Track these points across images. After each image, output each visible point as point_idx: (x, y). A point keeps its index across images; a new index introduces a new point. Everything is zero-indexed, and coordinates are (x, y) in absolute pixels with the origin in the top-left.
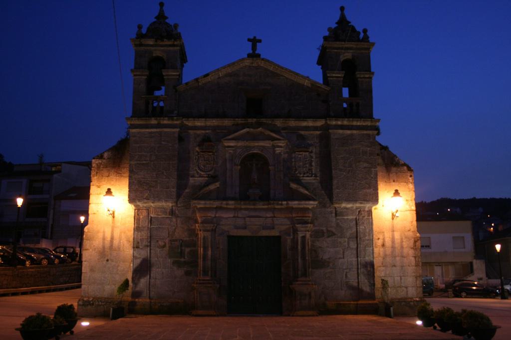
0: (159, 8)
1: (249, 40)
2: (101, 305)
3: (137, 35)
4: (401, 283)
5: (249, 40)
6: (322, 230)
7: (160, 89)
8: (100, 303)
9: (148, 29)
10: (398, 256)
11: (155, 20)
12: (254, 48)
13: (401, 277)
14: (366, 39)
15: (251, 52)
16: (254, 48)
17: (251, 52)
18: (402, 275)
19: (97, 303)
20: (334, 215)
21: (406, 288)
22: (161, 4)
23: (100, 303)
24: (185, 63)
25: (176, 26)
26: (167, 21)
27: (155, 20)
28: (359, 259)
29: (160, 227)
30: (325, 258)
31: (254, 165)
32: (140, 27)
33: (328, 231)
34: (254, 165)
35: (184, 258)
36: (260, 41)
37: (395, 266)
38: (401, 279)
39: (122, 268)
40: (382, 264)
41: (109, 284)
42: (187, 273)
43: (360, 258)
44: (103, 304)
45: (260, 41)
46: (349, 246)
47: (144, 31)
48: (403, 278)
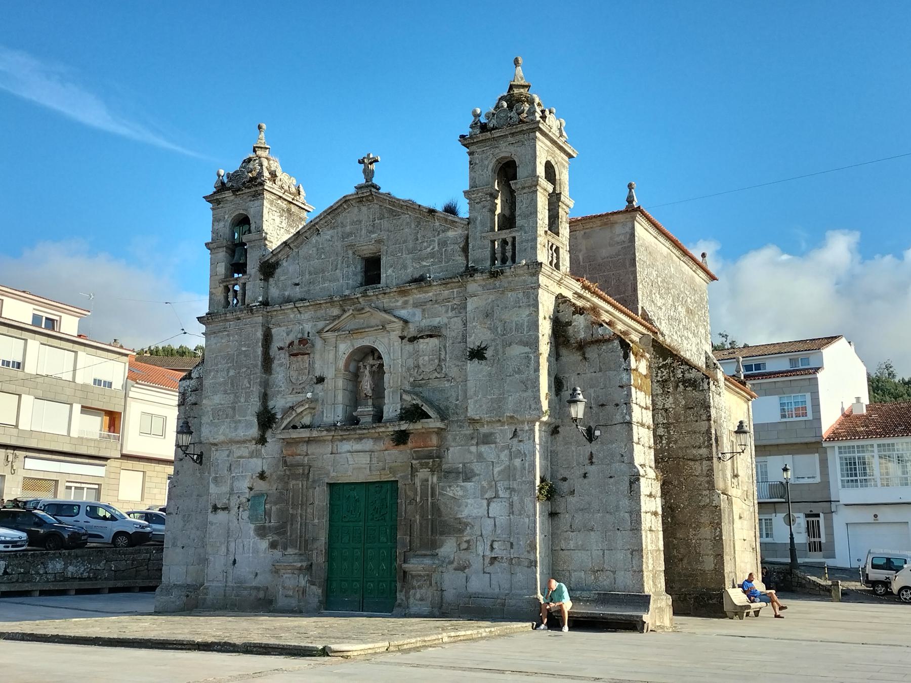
12: (369, 174)
17: (362, 181)
18: (606, 548)
20: (474, 442)
21: (614, 572)
29: (242, 476)
38: (603, 554)
42: (273, 545)
46: (497, 496)
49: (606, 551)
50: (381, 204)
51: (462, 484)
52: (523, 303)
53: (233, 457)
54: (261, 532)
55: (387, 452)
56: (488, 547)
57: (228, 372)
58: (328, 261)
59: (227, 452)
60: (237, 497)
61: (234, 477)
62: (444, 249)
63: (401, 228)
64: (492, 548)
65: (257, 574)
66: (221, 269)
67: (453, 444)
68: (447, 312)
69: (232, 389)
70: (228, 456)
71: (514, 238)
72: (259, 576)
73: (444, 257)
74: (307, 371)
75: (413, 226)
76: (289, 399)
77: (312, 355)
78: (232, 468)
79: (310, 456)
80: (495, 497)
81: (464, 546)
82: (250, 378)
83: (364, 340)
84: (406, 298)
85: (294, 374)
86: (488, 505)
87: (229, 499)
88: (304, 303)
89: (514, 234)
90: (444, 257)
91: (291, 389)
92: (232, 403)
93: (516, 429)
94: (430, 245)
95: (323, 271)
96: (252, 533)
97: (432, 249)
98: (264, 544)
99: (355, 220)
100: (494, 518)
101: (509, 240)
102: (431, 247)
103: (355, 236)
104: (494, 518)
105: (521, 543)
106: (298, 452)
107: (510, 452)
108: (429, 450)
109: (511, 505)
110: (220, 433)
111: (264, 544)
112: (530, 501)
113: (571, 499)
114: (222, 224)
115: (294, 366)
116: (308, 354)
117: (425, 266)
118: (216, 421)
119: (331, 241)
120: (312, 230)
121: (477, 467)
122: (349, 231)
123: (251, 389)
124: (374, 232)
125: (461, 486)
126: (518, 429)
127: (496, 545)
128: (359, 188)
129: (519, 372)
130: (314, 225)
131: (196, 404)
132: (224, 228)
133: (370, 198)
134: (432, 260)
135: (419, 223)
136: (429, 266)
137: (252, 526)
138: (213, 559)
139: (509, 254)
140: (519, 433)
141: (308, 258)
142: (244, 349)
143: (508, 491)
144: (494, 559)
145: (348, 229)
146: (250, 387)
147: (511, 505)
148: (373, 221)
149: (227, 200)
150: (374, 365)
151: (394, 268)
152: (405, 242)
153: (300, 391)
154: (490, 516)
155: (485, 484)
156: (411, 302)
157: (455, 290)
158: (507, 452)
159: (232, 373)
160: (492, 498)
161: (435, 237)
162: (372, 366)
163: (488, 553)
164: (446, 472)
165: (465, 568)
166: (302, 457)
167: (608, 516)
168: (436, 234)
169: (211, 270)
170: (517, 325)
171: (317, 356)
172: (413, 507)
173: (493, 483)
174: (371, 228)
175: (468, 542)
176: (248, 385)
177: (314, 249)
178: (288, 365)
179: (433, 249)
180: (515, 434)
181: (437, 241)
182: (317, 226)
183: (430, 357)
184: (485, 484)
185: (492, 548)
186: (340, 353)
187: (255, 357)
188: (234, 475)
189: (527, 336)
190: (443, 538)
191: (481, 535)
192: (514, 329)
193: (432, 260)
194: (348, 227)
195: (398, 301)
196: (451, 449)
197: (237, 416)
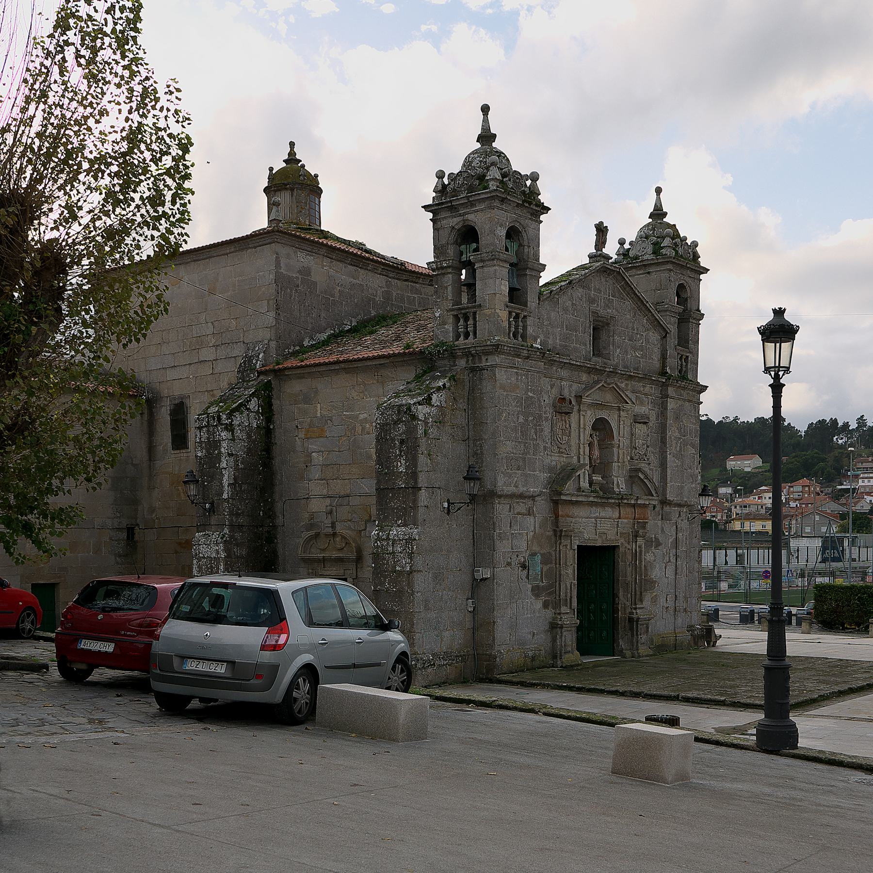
2: (444, 665)
35: (543, 582)
42: (546, 605)
46: (670, 561)
54: (536, 591)
71: (687, 357)
82: (536, 429)
87: (511, 558)
98: (539, 605)
137: (530, 586)
144: (667, 608)
179: (642, 343)
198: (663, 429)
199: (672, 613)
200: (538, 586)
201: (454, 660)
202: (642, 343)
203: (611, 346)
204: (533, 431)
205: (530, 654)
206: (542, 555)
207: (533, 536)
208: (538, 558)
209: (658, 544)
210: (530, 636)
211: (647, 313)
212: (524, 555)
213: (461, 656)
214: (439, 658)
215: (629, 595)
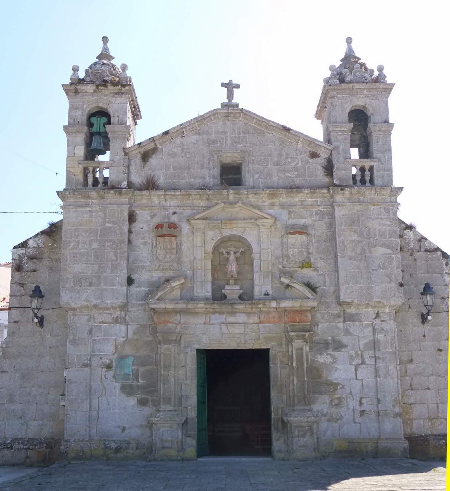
0: (102, 44)
1: (223, 85)
2: (23, 449)
3: (71, 79)
4: (438, 412)
5: (223, 85)
6: (327, 340)
7: (103, 153)
8: (22, 446)
9: (87, 71)
10: (432, 375)
11: (97, 60)
12: (230, 95)
13: (437, 404)
14: (379, 80)
15: (226, 101)
16: (230, 95)
17: (226, 101)
18: (439, 401)
19: (17, 446)
20: (341, 320)
22: (105, 39)
23: (22, 446)
24: (138, 119)
25: (124, 67)
26: (113, 62)
27: (97, 60)
28: (378, 379)
29: (104, 340)
30: (330, 378)
31: (232, 253)
32: (75, 69)
33: (333, 340)
34: (232, 253)
35: (138, 381)
36: (238, 86)
37: (429, 389)
38: (438, 406)
39: (53, 397)
40: (411, 386)
41: (34, 420)
42: (142, 403)
43: (379, 377)
44: (26, 447)
45: (238, 86)
46: (363, 362)
47: (81, 75)
48: (440, 405)
49: (439, 404)
50: (246, 122)
51: (332, 353)
52: (384, 215)
53: (95, 322)
54: (128, 390)
55: (261, 325)
56: (358, 402)
57: (91, 246)
58: (194, 160)
59: (87, 317)
60: (99, 359)
61: (95, 340)
62: (306, 167)
63: (266, 144)
64: (361, 403)
65: (124, 429)
66: (80, 151)
67: (322, 321)
68: (311, 215)
69: (95, 259)
70: (88, 321)
72: (127, 431)
73: (307, 172)
74: (174, 251)
75: (277, 144)
76: (154, 275)
77: (179, 238)
78: (93, 332)
79: (183, 325)
80: (362, 364)
81: (336, 402)
82: (116, 252)
83: (232, 230)
84: (272, 201)
85: (160, 253)
86: (356, 370)
87: (90, 360)
88: (175, 192)
89: (372, 163)
90: (307, 172)
91: (158, 266)
92: (96, 273)
93: (378, 312)
94: (294, 161)
95: (188, 168)
96: (118, 391)
97: (296, 165)
98: (132, 401)
99: (220, 130)
100: (362, 380)
101: (367, 168)
102: (295, 163)
103: (221, 144)
104: (362, 380)
105: (387, 399)
106: (171, 320)
107: (374, 329)
108: (304, 325)
109: (376, 370)
110: (83, 299)
111: (132, 401)
112: (394, 367)
113: (411, 367)
114: (79, 113)
115: (161, 245)
116: (176, 236)
117: (290, 177)
118: (78, 288)
119: (196, 144)
120: (179, 132)
121: (345, 340)
122: (214, 138)
123: (119, 261)
124: (239, 143)
125: (331, 355)
126: (380, 311)
127: (364, 401)
128: (223, 105)
129: (384, 268)
130: (182, 128)
131: (34, 271)
132: (82, 116)
133: (238, 115)
134: (296, 173)
135: (282, 143)
136: (293, 177)
137: (118, 385)
138: (74, 415)
139: (367, 178)
140: (382, 315)
141: (173, 155)
142: (108, 225)
143: (373, 359)
145: (213, 137)
146: (117, 260)
147: (376, 370)
148: (238, 134)
149: (87, 92)
150: (238, 252)
151: (260, 175)
152: (270, 155)
153: (168, 267)
154: (358, 378)
155: (353, 353)
156: (277, 203)
157: (318, 199)
158: (370, 328)
159: (95, 245)
160: (359, 365)
161: (298, 155)
162: (235, 253)
163: (358, 407)
164: (317, 343)
165: (337, 420)
166: (175, 325)
167: (440, 378)
168: (299, 154)
169: (68, 151)
170: (380, 232)
171: (184, 239)
172: (287, 370)
173: (360, 353)
174: (236, 140)
175: (339, 398)
176: (114, 258)
177: (180, 149)
178: (154, 244)
180: (378, 315)
181: (300, 159)
182: (184, 130)
183: (299, 250)
184: (353, 353)
185: (361, 403)
186: (208, 239)
187: (121, 233)
188: (95, 338)
189: (389, 241)
190: (317, 396)
191: (351, 393)
192: (378, 235)
193: (296, 173)
194: (213, 136)
195: (265, 202)
196: (320, 325)
197: (102, 285)
198: (333, 237)
199: (373, 416)
200: (131, 386)
201: (36, 445)
202: (297, 164)
203: (247, 174)
204: (112, 253)
205: (113, 445)
206: (134, 358)
207: (125, 342)
208: (129, 361)
209: (339, 346)
210: (119, 430)
211: (297, 138)
212: (111, 357)
213: (46, 443)
214: (18, 442)
215: (284, 397)
